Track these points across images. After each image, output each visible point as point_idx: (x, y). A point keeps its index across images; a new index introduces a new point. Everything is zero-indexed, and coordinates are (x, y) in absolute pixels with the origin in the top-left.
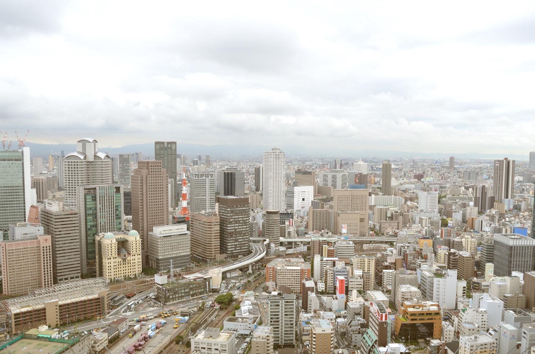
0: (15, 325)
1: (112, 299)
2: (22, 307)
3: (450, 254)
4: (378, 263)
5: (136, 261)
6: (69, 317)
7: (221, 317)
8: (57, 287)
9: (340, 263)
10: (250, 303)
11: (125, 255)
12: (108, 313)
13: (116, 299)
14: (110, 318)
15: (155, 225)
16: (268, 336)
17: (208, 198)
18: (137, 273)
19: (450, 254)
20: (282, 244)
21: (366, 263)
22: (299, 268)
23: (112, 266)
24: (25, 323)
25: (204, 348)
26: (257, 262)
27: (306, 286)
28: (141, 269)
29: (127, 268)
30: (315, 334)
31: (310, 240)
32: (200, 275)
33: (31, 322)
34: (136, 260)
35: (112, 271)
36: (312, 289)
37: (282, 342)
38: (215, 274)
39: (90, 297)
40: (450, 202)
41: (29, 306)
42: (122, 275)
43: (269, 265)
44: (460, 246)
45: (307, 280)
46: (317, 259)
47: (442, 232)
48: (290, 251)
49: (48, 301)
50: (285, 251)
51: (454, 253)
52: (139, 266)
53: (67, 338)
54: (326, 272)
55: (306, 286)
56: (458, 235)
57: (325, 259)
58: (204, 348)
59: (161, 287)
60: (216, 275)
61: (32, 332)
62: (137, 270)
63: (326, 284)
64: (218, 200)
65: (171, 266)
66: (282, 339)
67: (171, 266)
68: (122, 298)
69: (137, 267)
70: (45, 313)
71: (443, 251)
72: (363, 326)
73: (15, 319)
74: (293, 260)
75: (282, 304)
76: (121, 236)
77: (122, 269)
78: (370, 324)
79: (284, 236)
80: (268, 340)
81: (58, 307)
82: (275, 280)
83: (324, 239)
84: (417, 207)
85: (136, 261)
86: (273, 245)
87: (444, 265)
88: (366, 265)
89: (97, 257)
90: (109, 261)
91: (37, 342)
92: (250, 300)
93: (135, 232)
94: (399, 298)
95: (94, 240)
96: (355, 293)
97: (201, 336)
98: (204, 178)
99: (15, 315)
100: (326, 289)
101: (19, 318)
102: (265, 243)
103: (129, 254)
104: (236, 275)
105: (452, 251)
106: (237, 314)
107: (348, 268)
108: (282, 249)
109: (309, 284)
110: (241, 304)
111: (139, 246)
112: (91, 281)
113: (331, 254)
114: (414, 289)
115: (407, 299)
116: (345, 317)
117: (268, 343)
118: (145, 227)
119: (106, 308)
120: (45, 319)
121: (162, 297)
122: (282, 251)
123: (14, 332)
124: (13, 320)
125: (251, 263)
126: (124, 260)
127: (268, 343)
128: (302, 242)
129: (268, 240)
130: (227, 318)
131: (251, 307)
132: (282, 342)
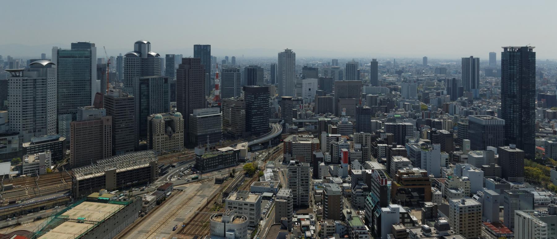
0: (79, 190)
1: (160, 168)
2: (86, 175)
3: (432, 132)
4: (373, 139)
5: (180, 137)
6: (124, 183)
7: (248, 183)
8: (115, 158)
11: (171, 133)
12: (157, 179)
13: (164, 168)
14: (159, 183)
15: (195, 108)
16: (288, 197)
17: (235, 87)
19: (432, 132)
20: (295, 124)
21: (364, 138)
22: (310, 142)
23: (160, 141)
24: (88, 188)
25: (236, 208)
26: (275, 138)
27: (317, 157)
29: (172, 143)
30: (327, 196)
31: (317, 121)
32: (231, 148)
33: (93, 187)
34: (180, 135)
35: (160, 145)
36: (321, 160)
37: (299, 203)
38: (242, 146)
39: (142, 166)
40: (426, 92)
41: (91, 174)
42: (168, 148)
43: (286, 140)
44: (439, 125)
45: (317, 152)
46: (324, 135)
47: (423, 115)
48: (302, 129)
49: (107, 169)
50: (297, 129)
51: (435, 131)
53: (122, 200)
54: (332, 145)
55: (317, 157)
56: (437, 117)
58: (236, 208)
60: (243, 148)
61: (95, 195)
62: (180, 144)
63: (332, 156)
64: (245, 89)
65: (208, 141)
66: (299, 200)
67: (208, 141)
68: (168, 167)
69: (180, 142)
70: (105, 179)
71: (426, 130)
72: (365, 190)
73: (79, 185)
74: (305, 136)
75: (299, 170)
76: (168, 117)
77: (168, 144)
78: (372, 187)
79: (296, 118)
80: (289, 201)
81: (116, 175)
82: (291, 153)
83: (329, 119)
84: (400, 96)
85: (180, 137)
86: (287, 124)
87: (428, 140)
88: (364, 140)
89: (148, 134)
90: (158, 137)
91: (96, 204)
93: (178, 113)
94: (393, 167)
95: (146, 121)
96: (356, 163)
97: (233, 197)
98: (232, 72)
99: (80, 181)
100: (332, 160)
101: (83, 184)
102: (281, 123)
103: (174, 131)
104: (259, 148)
105: (433, 129)
106: (261, 179)
107: (349, 142)
108: (294, 127)
109: (319, 155)
110: (264, 172)
111: (182, 125)
112: (143, 153)
113: (334, 131)
114: (405, 160)
115: (400, 168)
116: (349, 183)
117: (289, 203)
118: (187, 110)
119: (155, 175)
120: (105, 185)
121: (201, 167)
122: (295, 129)
123: (78, 196)
124: (78, 186)
125: (271, 139)
126: (170, 136)
127: (289, 203)
128: (310, 122)
130: (253, 183)
131: (272, 174)
132: (299, 203)
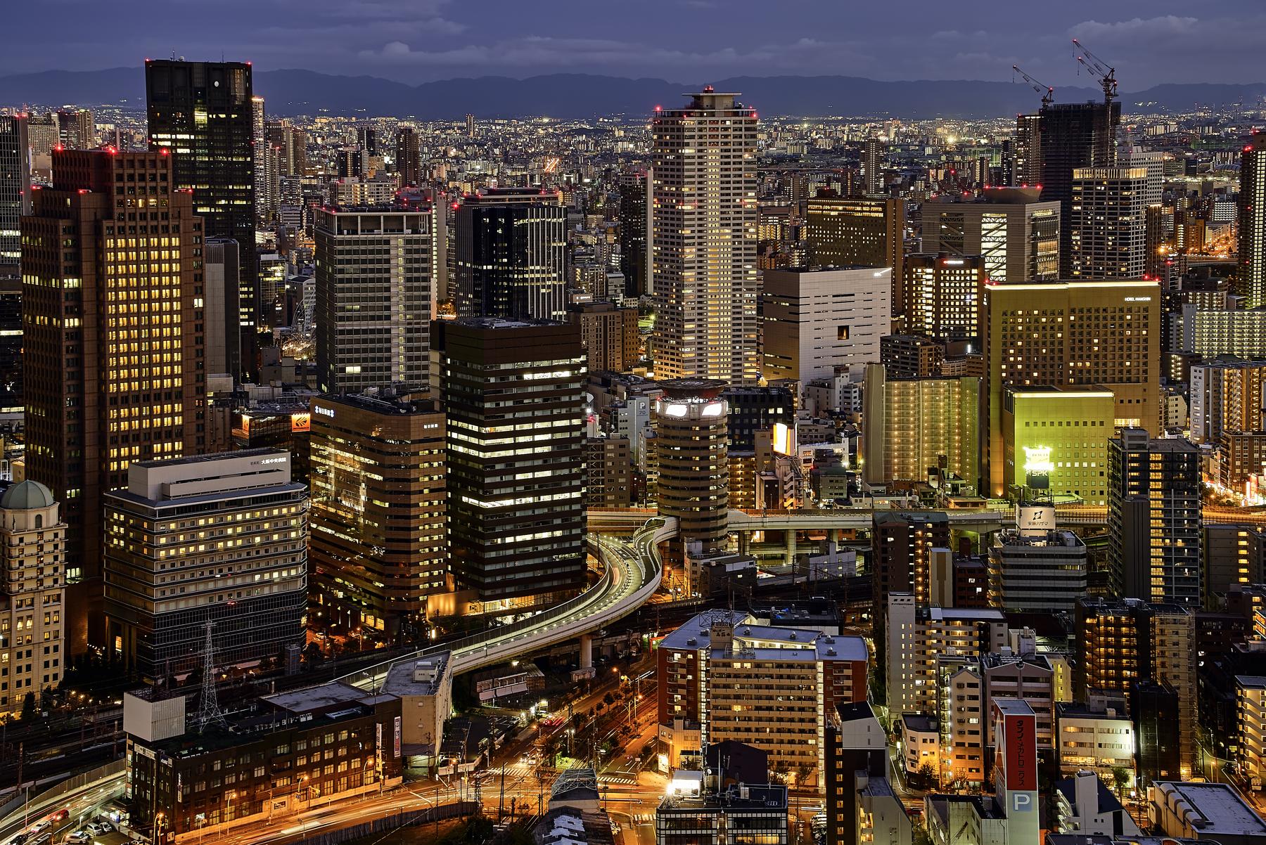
9: (1014, 633)
10: (579, 825)
18: (36, 689)
28: (60, 671)
52: (51, 657)
57: (937, 613)
59: (151, 754)
65: (209, 650)
67: (209, 650)
69: (38, 659)
92: (577, 813)
104: (522, 687)
125: (593, 634)
129: (670, 523)
